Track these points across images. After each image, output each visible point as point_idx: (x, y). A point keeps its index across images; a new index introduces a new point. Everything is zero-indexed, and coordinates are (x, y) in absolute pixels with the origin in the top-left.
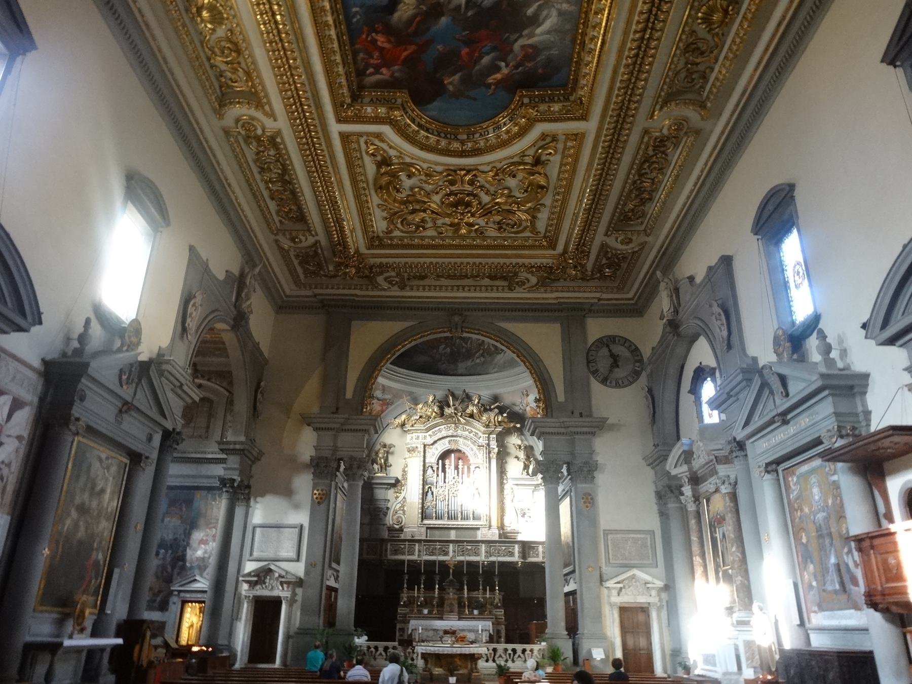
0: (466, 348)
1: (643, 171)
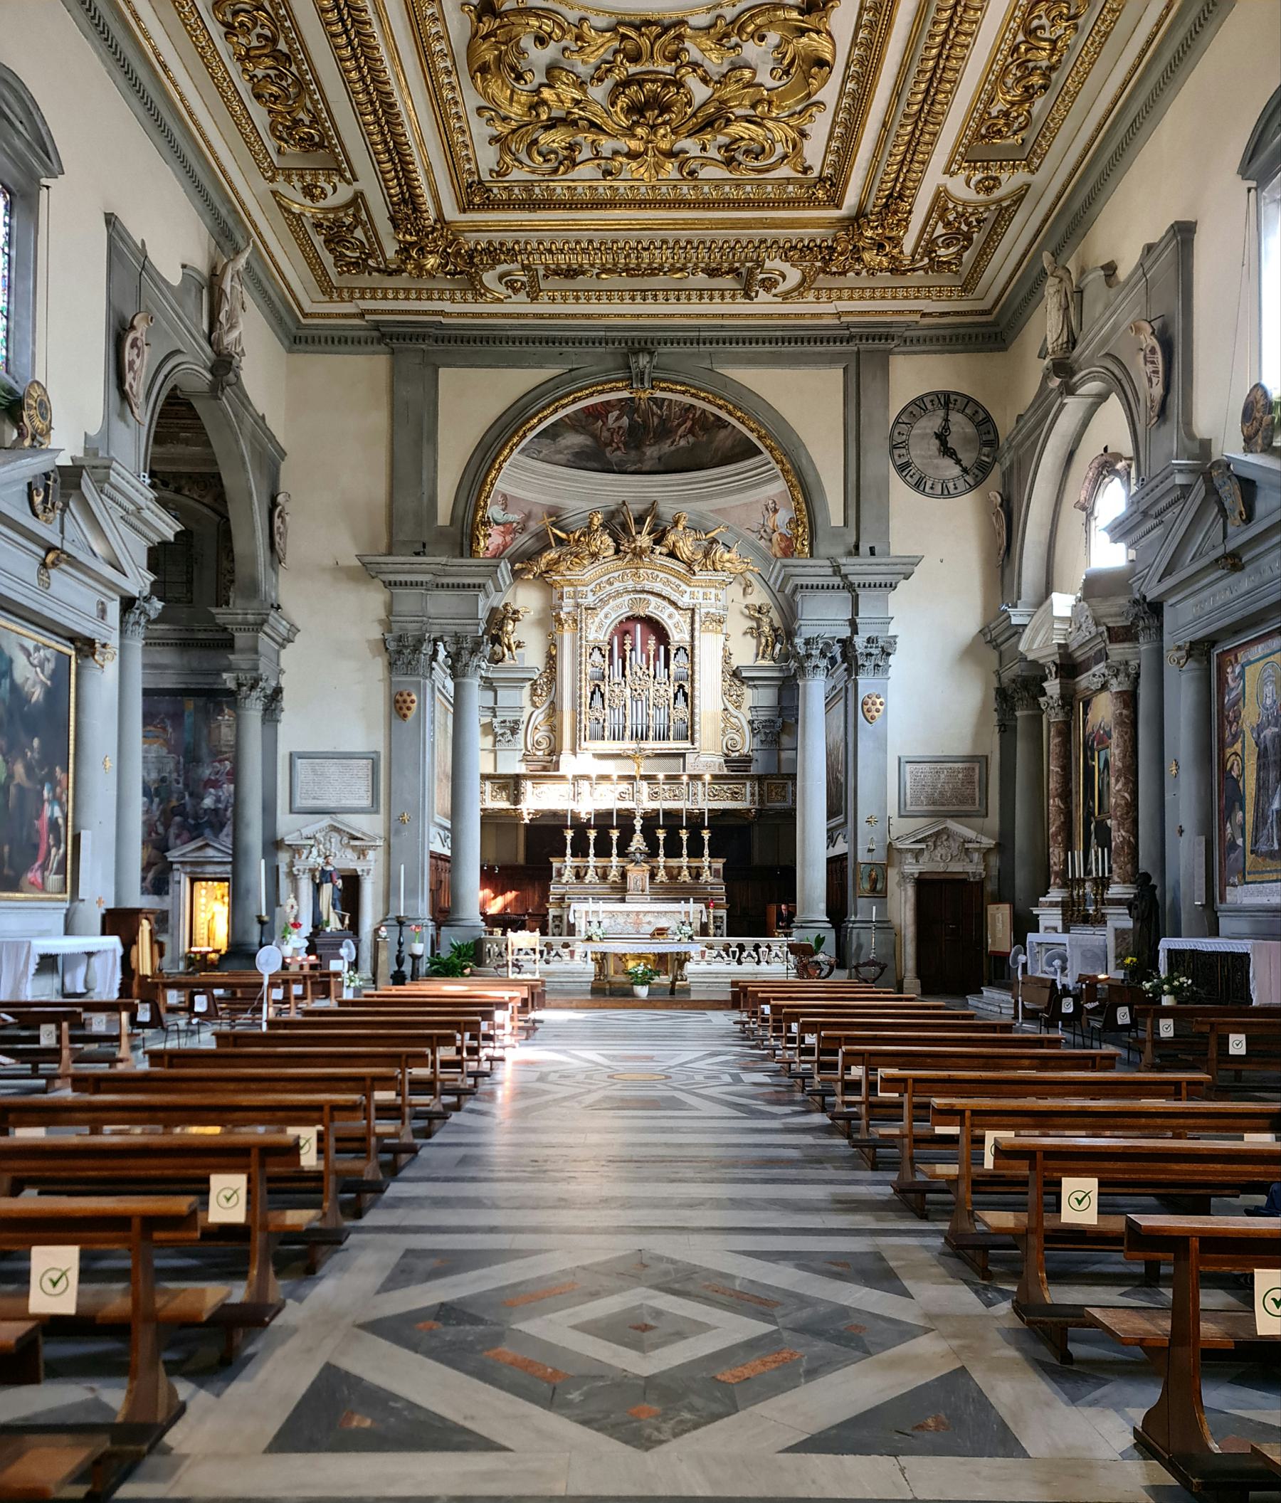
0: (660, 417)
1: (1035, 23)
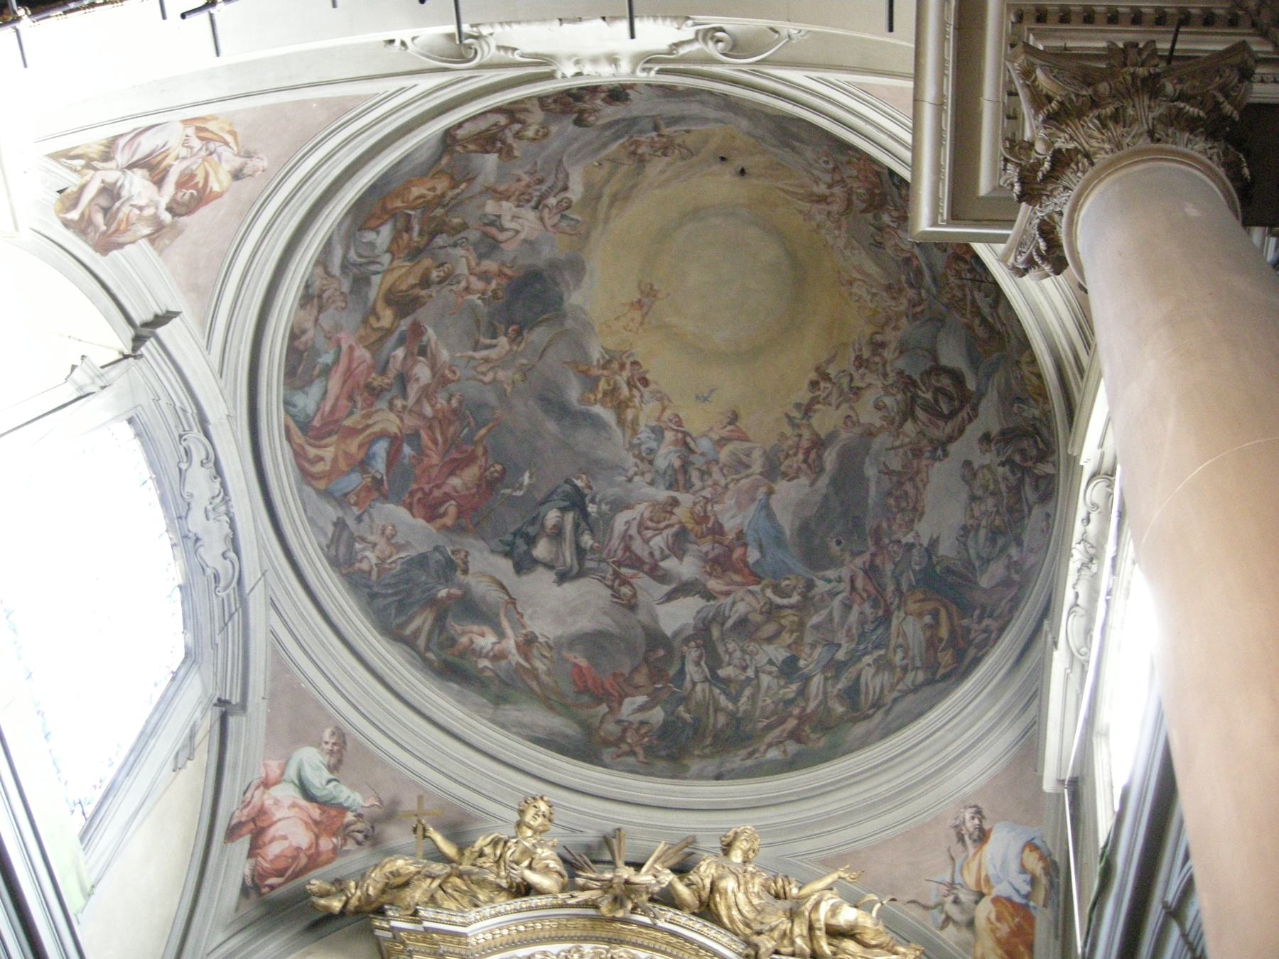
0: (732, 715)
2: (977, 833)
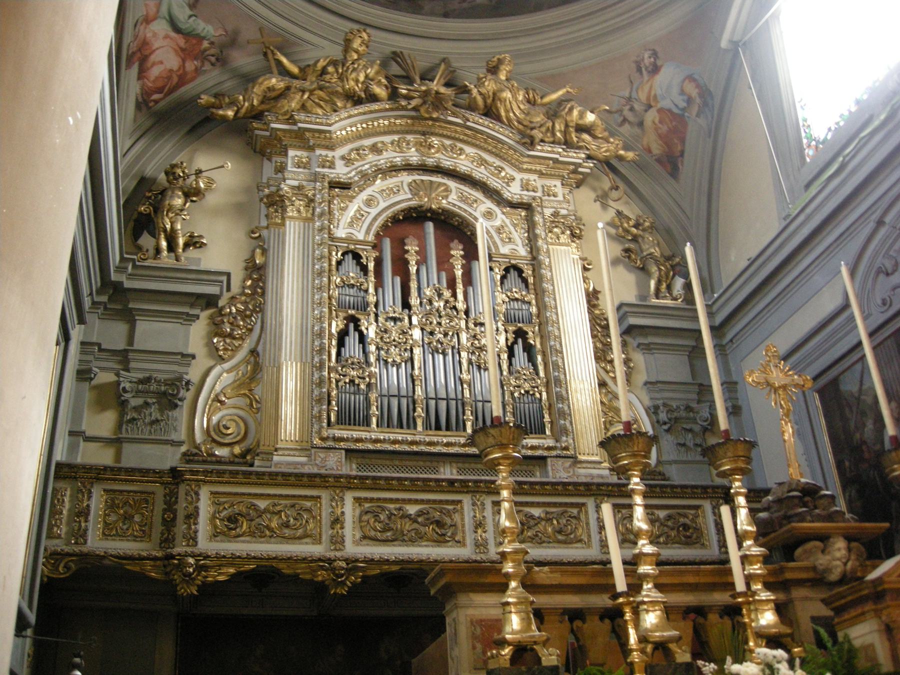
2: (651, 67)
